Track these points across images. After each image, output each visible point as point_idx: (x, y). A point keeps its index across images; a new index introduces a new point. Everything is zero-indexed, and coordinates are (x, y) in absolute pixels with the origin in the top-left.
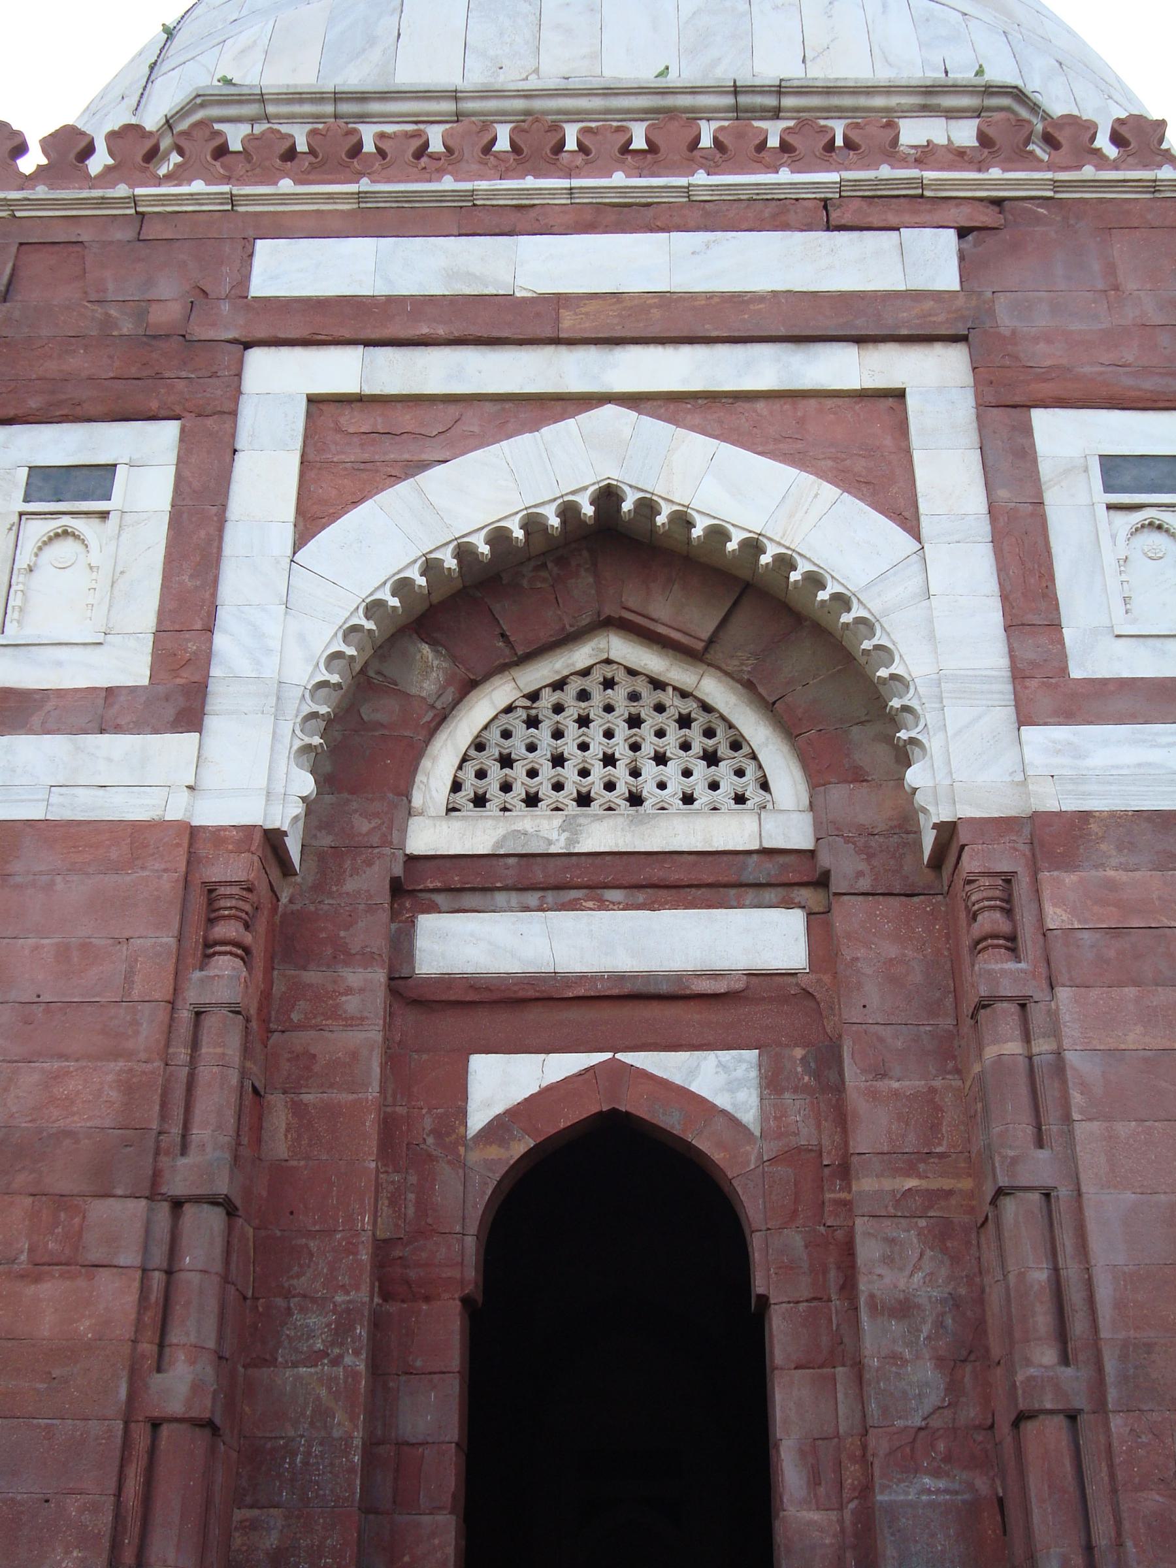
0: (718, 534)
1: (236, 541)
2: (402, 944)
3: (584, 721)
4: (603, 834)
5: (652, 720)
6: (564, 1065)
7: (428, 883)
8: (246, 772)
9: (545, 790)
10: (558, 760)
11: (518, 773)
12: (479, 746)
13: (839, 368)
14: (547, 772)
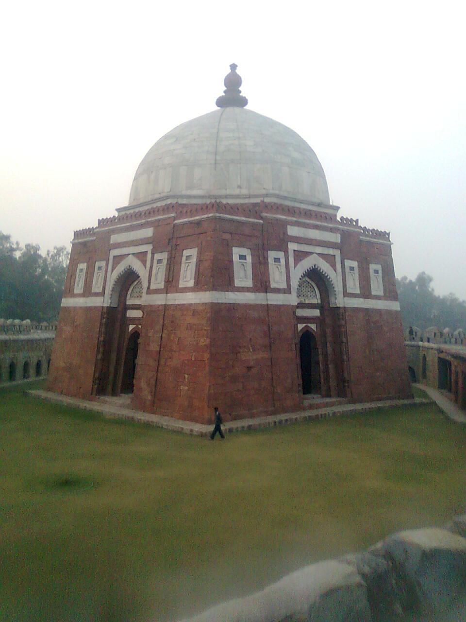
7: (126, 308)
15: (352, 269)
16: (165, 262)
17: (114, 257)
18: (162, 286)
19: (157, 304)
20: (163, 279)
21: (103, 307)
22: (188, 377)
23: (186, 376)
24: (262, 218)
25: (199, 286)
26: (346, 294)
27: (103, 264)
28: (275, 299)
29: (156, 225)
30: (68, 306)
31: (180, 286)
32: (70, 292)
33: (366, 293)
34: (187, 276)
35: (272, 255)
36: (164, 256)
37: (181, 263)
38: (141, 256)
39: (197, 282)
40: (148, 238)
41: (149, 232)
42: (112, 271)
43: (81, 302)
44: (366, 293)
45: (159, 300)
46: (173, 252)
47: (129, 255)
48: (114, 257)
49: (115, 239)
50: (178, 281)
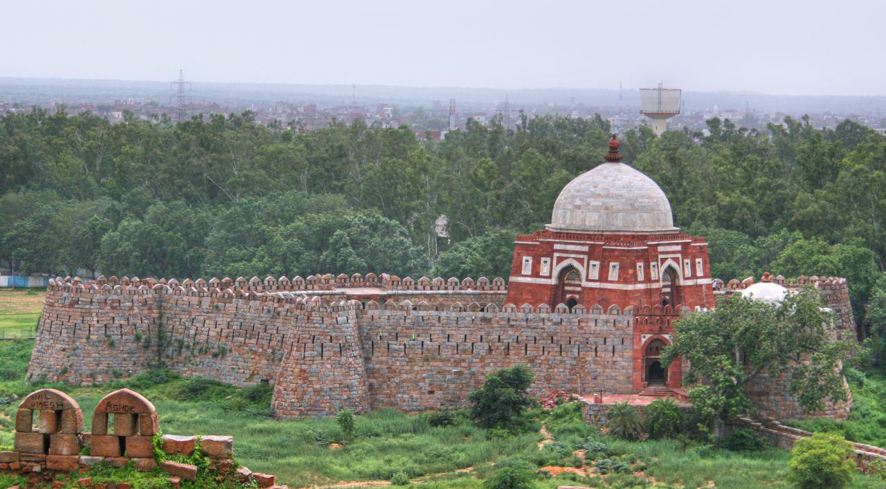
2: (563, 288)
4: (573, 283)
7: (565, 285)
8: (553, 281)
13: (581, 256)
15: (687, 264)
24: (648, 245)
25: (623, 279)
26: (685, 279)
27: (548, 259)
28: (655, 286)
29: (592, 246)
32: (518, 272)
33: (694, 276)
34: (613, 274)
35: (653, 263)
38: (581, 261)
39: (620, 277)
41: (586, 249)
43: (529, 280)
44: (694, 276)
45: (597, 285)
49: (556, 247)
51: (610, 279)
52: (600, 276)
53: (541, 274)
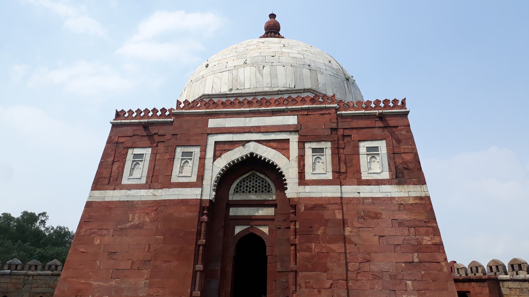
0: (265, 159)
1: (206, 161)
3: (250, 181)
5: (259, 181)
6: (246, 227)
9: (245, 190)
10: (247, 187)
11: (242, 188)
12: (238, 185)
14: (245, 188)
16: (328, 152)
17: (215, 142)
18: (329, 176)
19: (324, 195)
20: (330, 168)
21: (201, 200)
22: (412, 285)
23: (409, 282)
27: (196, 151)
30: (107, 199)
31: (363, 178)
36: (327, 146)
37: (358, 154)
40: (289, 126)
41: (292, 120)
42: (214, 160)
45: (331, 192)
46: (341, 142)
47: (251, 141)
48: (215, 142)
50: (359, 172)
51: (365, 176)
52: (337, 172)
53: (174, 179)
